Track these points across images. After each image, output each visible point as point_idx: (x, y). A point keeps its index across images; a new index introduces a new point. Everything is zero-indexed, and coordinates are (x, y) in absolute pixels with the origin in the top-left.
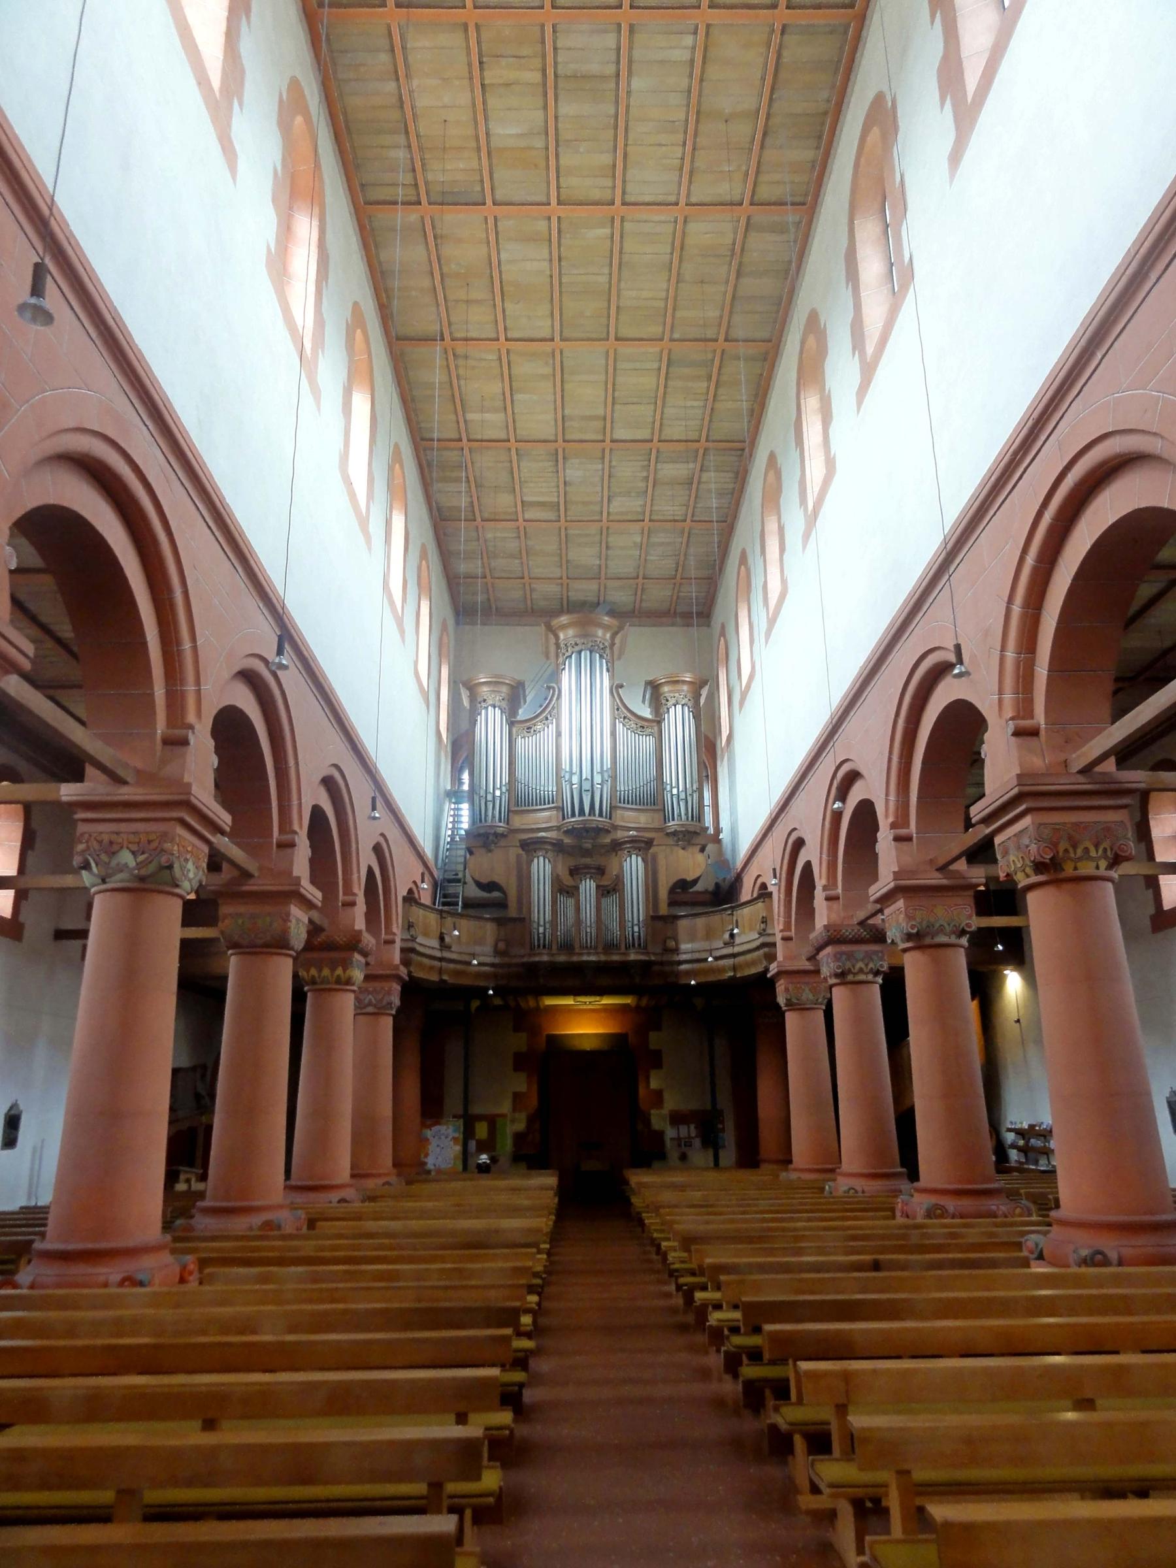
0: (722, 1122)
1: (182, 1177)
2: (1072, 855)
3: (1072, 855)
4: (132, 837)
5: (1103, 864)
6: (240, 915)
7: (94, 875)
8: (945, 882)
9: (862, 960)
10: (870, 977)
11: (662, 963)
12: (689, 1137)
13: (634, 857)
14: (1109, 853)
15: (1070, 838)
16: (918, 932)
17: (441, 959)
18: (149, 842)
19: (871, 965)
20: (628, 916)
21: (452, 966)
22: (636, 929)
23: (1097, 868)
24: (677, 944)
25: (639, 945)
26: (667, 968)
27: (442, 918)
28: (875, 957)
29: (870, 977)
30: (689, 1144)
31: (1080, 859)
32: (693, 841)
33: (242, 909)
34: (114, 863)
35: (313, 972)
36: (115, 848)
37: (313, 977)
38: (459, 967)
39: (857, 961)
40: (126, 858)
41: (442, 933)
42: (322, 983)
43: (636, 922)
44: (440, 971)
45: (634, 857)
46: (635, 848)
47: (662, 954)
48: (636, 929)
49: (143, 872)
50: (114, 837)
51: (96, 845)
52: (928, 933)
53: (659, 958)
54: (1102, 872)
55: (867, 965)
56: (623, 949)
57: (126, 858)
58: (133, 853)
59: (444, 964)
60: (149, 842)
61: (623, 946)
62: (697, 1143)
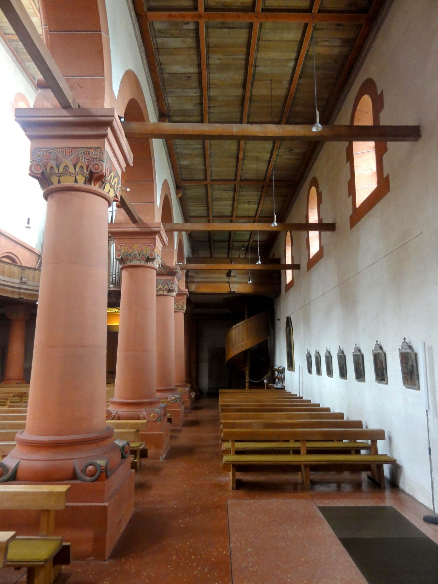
2: (57, 171)
3: (57, 171)
5: (81, 179)
8: (137, 230)
9: (162, 284)
10: (166, 293)
14: (85, 171)
15: (57, 159)
16: (122, 258)
17: (20, 288)
19: (166, 286)
20: (111, 271)
21: (28, 292)
23: (76, 181)
25: (115, 284)
27: (22, 270)
28: (169, 283)
29: (166, 293)
31: (61, 175)
38: (32, 292)
39: (159, 284)
41: (22, 277)
44: (20, 294)
48: (114, 276)
52: (128, 259)
54: (81, 184)
55: (164, 287)
59: (22, 291)
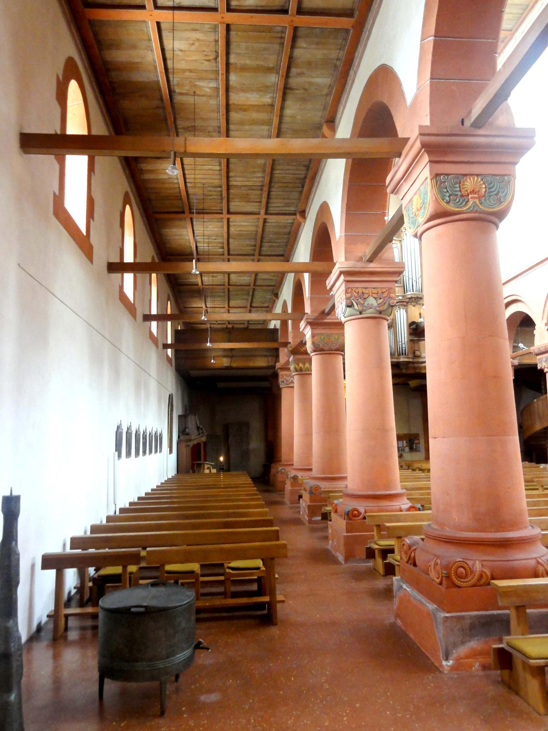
0: (419, 440)
1: (206, 466)
4: (375, 291)
6: (322, 334)
7: (355, 310)
11: (413, 363)
12: (403, 447)
13: (402, 310)
18: (383, 293)
22: (404, 346)
24: (420, 353)
26: (416, 365)
30: (403, 450)
32: (419, 303)
33: (323, 331)
34: (366, 304)
35: (301, 365)
36: (366, 296)
37: (301, 368)
40: (371, 301)
42: (305, 371)
43: (403, 342)
45: (402, 310)
46: (402, 305)
47: (413, 358)
49: (381, 308)
50: (364, 291)
51: (355, 294)
53: (411, 360)
56: (396, 356)
57: (371, 301)
58: (375, 298)
60: (383, 293)
61: (396, 354)
62: (407, 449)
